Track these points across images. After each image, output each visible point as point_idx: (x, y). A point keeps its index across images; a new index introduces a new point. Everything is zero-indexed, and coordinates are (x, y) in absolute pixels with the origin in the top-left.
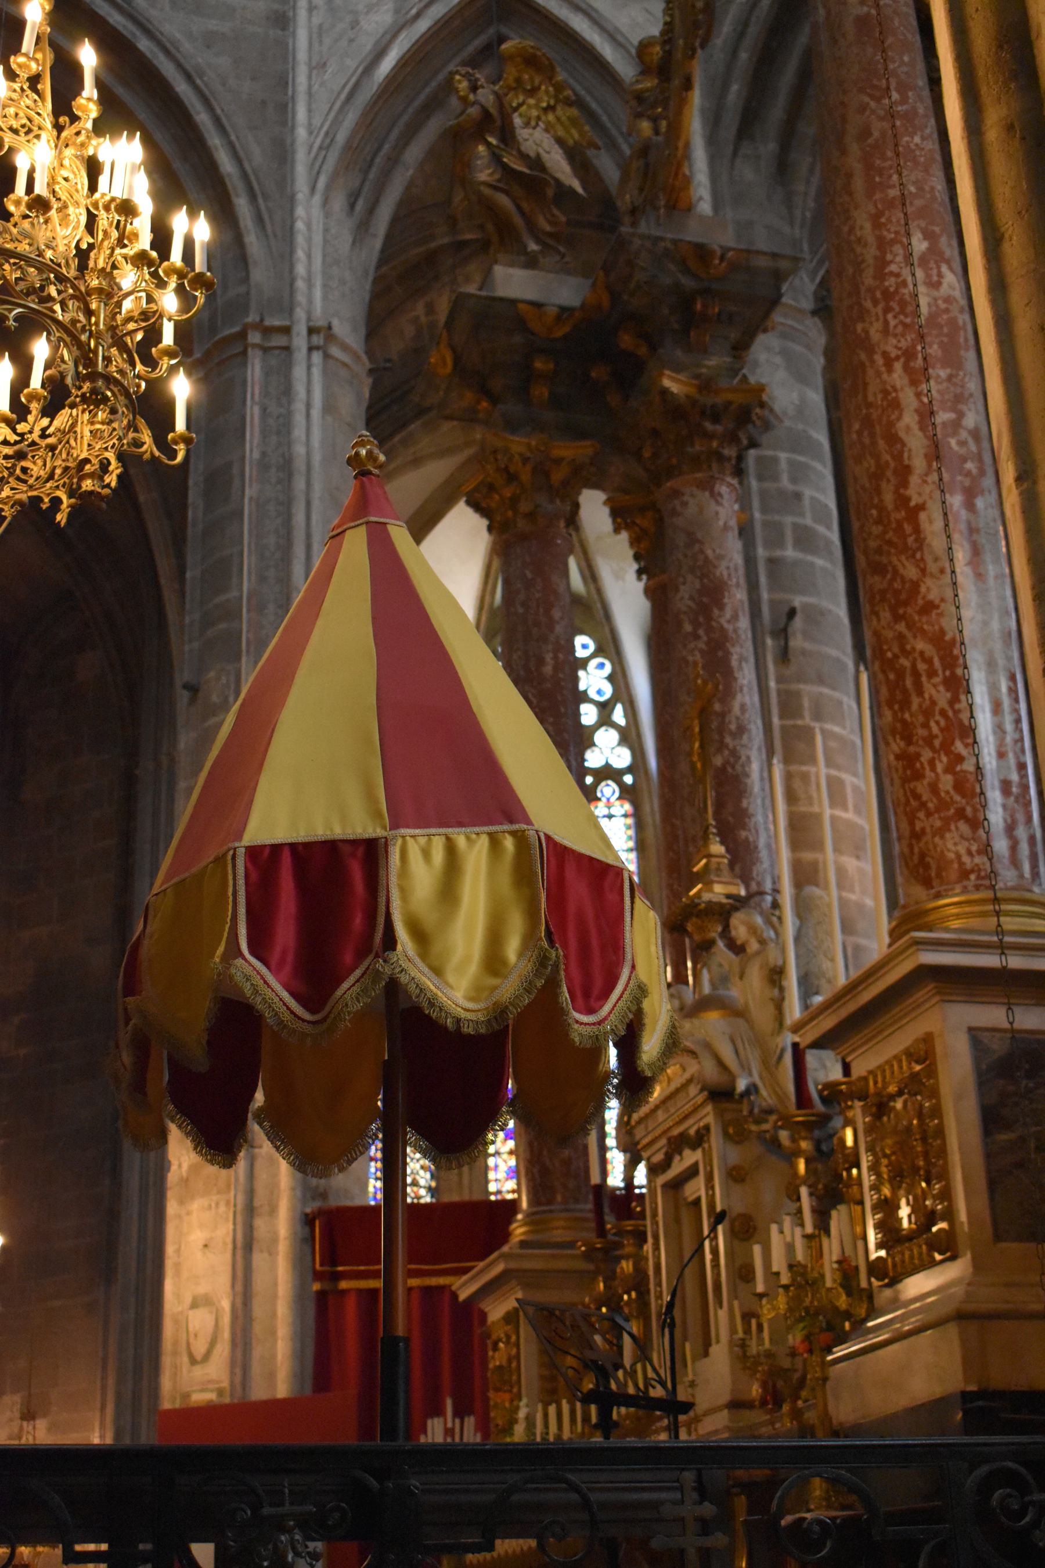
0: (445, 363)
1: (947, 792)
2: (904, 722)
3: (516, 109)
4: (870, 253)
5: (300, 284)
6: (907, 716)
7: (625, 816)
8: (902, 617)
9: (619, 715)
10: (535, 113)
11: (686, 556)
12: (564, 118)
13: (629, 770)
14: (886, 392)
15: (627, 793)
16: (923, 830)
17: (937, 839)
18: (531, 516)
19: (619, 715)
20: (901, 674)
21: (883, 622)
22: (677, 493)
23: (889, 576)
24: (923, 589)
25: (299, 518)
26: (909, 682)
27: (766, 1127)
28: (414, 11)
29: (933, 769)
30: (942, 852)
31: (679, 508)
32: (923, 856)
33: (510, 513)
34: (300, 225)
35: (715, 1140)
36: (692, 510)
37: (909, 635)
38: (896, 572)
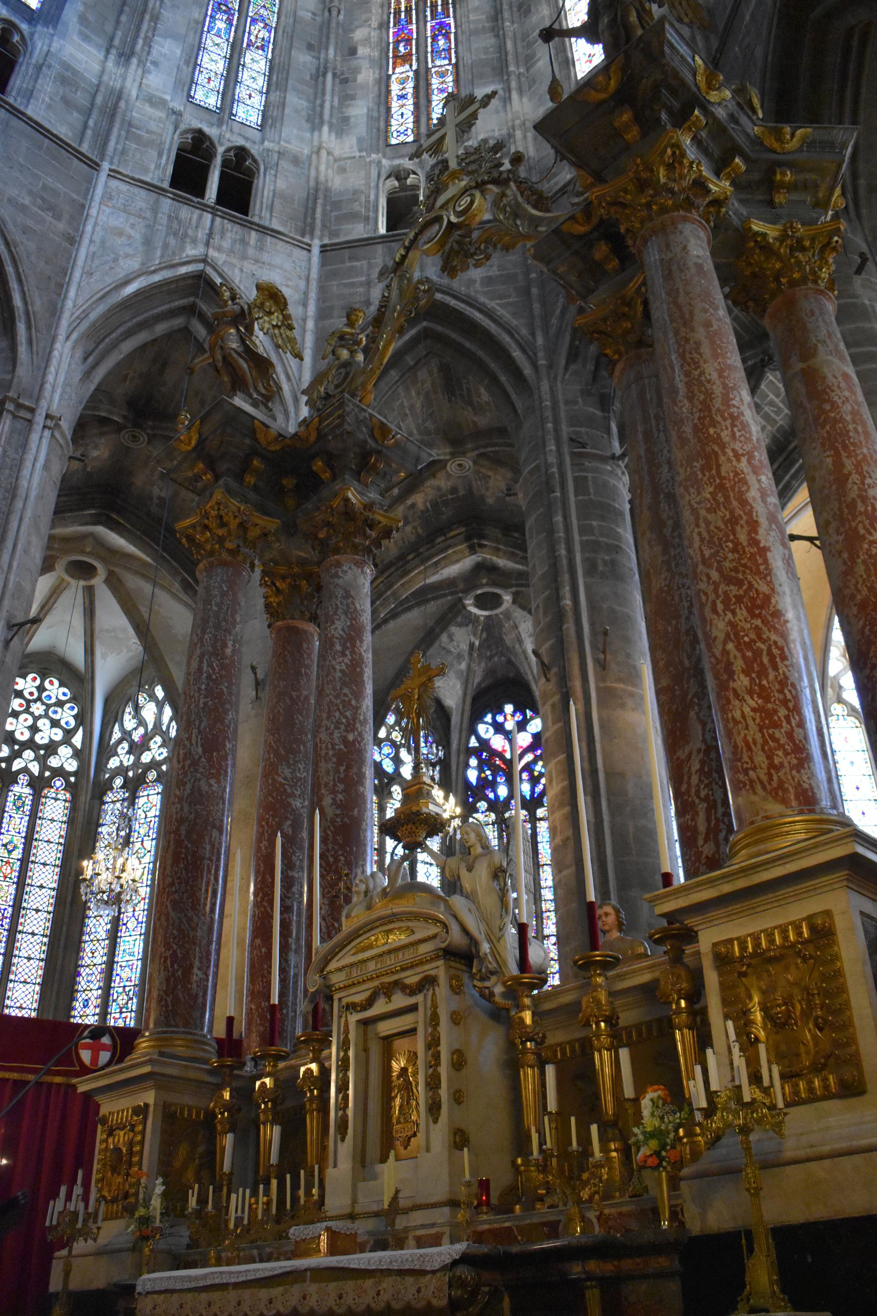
0: (190, 442)
1: (800, 741)
2: (761, 686)
3: (257, 319)
4: (718, 390)
5: (48, 387)
6: (764, 682)
7: (65, 801)
8: (759, 616)
9: (77, 740)
11: (342, 603)
13: (75, 774)
14: (737, 474)
15: (69, 787)
16: (782, 765)
17: (794, 772)
18: (231, 552)
19: (77, 740)
20: (758, 653)
21: (739, 616)
22: (338, 564)
23: (745, 587)
24: (773, 601)
25: (14, 524)
26: (765, 660)
27: (487, 984)
29: (789, 722)
30: (799, 782)
32: (781, 782)
33: (217, 546)
34: (56, 353)
35: (442, 990)
36: (349, 577)
37: (765, 629)
38: (751, 585)
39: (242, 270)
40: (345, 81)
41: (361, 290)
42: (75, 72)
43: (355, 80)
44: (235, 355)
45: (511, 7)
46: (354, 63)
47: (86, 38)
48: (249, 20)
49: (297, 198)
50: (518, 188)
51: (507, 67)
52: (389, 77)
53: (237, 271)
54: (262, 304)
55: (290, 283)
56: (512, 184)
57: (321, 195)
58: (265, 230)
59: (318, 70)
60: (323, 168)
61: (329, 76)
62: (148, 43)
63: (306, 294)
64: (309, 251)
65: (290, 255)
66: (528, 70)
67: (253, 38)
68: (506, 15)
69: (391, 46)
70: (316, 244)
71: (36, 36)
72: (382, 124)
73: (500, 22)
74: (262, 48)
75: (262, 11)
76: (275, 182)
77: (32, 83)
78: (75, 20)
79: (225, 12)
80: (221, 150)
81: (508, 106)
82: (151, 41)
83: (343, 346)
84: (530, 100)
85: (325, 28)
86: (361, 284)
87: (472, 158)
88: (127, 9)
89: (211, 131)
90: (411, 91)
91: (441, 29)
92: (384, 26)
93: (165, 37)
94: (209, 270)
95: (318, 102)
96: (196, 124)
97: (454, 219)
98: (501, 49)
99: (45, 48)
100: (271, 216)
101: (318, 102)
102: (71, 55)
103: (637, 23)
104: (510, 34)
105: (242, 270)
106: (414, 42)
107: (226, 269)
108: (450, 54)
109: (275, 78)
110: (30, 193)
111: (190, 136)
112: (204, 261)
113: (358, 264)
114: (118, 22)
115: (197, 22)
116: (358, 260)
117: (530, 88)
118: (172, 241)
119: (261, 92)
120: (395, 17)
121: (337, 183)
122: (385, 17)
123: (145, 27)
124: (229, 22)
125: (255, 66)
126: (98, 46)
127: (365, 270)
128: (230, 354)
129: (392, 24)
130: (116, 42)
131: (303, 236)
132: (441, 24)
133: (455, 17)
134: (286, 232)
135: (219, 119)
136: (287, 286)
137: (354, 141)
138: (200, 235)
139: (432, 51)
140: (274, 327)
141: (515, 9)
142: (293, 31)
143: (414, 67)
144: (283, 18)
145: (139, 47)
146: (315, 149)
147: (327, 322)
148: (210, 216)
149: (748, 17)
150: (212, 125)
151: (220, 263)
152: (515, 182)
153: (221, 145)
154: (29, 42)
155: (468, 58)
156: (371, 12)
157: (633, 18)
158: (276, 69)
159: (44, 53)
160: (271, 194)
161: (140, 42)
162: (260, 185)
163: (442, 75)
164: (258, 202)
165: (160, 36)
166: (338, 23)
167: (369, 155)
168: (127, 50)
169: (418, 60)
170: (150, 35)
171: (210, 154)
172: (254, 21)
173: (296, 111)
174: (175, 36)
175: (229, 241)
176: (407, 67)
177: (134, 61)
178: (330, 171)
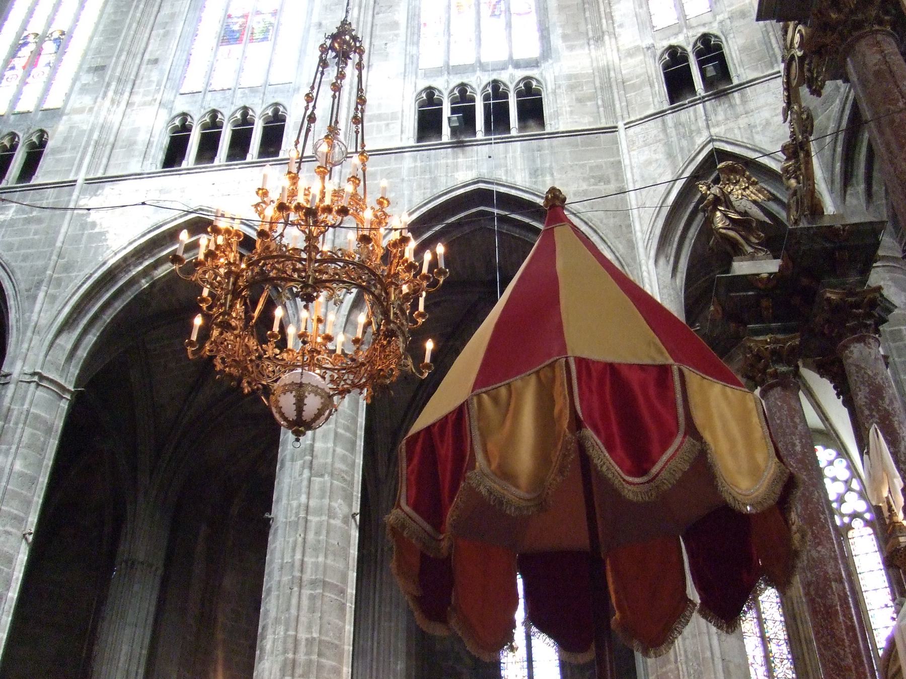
11: (858, 377)
12: (754, 191)
28: (680, 172)
31: (849, 355)
39: (739, 128)
42: (576, 76)
47: (571, 48)
49: (756, 42)
82: (611, 13)
105: (739, 128)
110: (584, 179)
111: (666, 56)
112: (712, 140)
114: (586, 19)
118: (684, 143)
126: (582, 46)
130: (591, 34)
138: (700, 125)
140: (744, 189)
154: (542, 80)
159: (553, 80)
170: (608, 10)
177: (606, 37)
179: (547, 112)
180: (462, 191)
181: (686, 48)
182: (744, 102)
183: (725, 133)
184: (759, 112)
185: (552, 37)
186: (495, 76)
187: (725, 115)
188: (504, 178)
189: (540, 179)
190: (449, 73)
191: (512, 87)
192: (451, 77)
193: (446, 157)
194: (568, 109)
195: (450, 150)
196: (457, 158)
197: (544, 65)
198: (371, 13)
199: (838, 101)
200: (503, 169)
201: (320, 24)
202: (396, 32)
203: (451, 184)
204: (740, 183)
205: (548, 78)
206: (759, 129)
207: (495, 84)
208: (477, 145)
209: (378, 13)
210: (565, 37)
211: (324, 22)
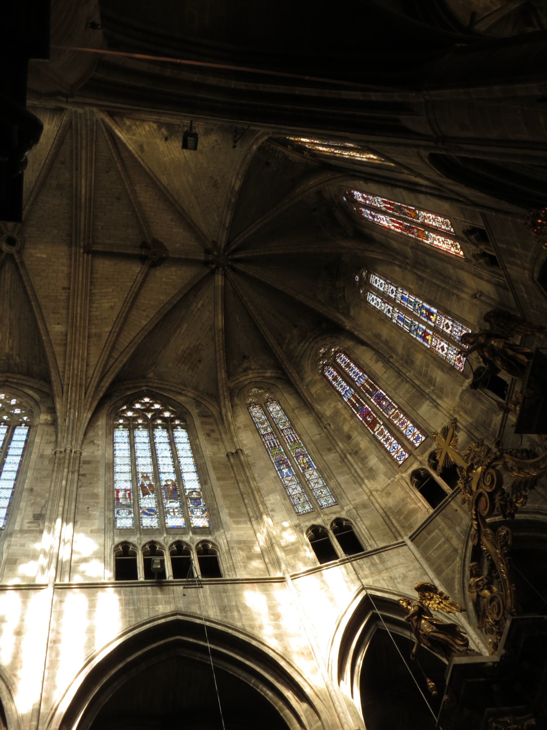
10: (435, 606)
12: (447, 604)
39: (384, 580)
40: (356, 453)
41: (446, 546)
43: (360, 449)
44: (435, 634)
45: (403, 366)
46: (354, 442)
47: (238, 523)
48: (295, 459)
49: (379, 523)
50: (511, 455)
51: (424, 392)
52: (374, 435)
53: (382, 581)
54: (424, 596)
55: (410, 568)
56: (505, 455)
57: (389, 514)
58: (377, 551)
59: (341, 456)
60: (379, 500)
61: (349, 456)
62: (264, 504)
63: (422, 567)
64: (406, 545)
65: (399, 554)
66: (434, 386)
67: (302, 465)
68: (404, 371)
69: (363, 422)
70: (406, 539)
71: (217, 538)
72: (389, 459)
73: (404, 376)
74: (310, 466)
75: (297, 450)
76: (364, 523)
77: (231, 562)
78: (228, 518)
79: (283, 463)
80: (328, 527)
81: (440, 408)
82: (263, 501)
83: (482, 590)
84: (447, 398)
85: (329, 436)
86: (444, 543)
87: (472, 456)
88: (244, 496)
89: (318, 522)
90: (389, 434)
91: (380, 398)
92: (353, 416)
93: (268, 495)
94: (370, 592)
95: (353, 471)
96: (309, 524)
97: (489, 490)
98: (414, 385)
99: (225, 541)
100: (375, 541)
101: (353, 471)
102: (237, 535)
103: (514, 353)
104: (413, 377)
106: (372, 413)
107: (376, 585)
108: (392, 405)
109: (325, 475)
111: (310, 532)
112: (363, 589)
113: (433, 534)
114: (245, 505)
115: (275, 478)
116: (433, 532)
117: (443, 393)
119: (324, 486)
120: (355, 409)
121: (391, 502)
122: (350, 411)
123: (257, 498)
124: (288, 466)
125: (313, 477)
126: (245, 522)
127: (440, 534)
128: (432, 636)
129: (356, 412)
130: (251, 514)
131: (397, 539)
132: (377, 396)
133: (381, 388)
134: (389, 544)
135: (317, 513)
136: (410, 571)
137: (383, 476)
139: (384, 410)
140: (439, 604)
141: (405, 365)
142: (317, 449)
143: (381, 423)
144: (308, 447)
145: (262, 509)
146: (369, 494)
147: (444, 574)
148: (349, 564)
149: (525, 296)
150: (315, 519)
151: (371, 584)
152: (507, 453)
153: (327, 525)
154: (217, 544)
155: (401, 401)
156: (343, 414)
157: (511, 353)
158: (323, 471)
160: (366, 530)
161: (261, 506)
162: (358, 530)
163: (397, 417)
164: (363, 538)
165: (266, 496)
166: (333, 430)
167: (394, 477)
168: (258, 514)
169: (380, 419)
170: (262, 500)
171: (325, 533)
172: (297, 457)
173: (347, 483)
174: (272, 491)
175: (367, 569)
176: (378, 425)
178: (384, 499)
179: (224, 565)
180: (163, 621)
181: (325, 526)
182: (382, 561)
183: (373, 583)
184: (396, 569)
185: (221, 514)
186: (177, 538)
187: (370, 571)
188: (198, 612)
189: (229, 614)
190: (140, 534)
191: (193, 547)
192: (142, 536)
193: (147, 593)
194: (242, 564)
195: (149, 588)
196: (156, 594)
197: (217, 534)
198: (75, 485)
199: (458, 559)
200: (197, 605)
201: (31, 490)
202: (97, 501)
203: (152, 615)
204: (434, 599)
205: (221, 541)
206: (399, 580)
207: (179, 544)
208: (173, 585)
209: (81, 487)
210: (231, 515)
211: (35, 488)
